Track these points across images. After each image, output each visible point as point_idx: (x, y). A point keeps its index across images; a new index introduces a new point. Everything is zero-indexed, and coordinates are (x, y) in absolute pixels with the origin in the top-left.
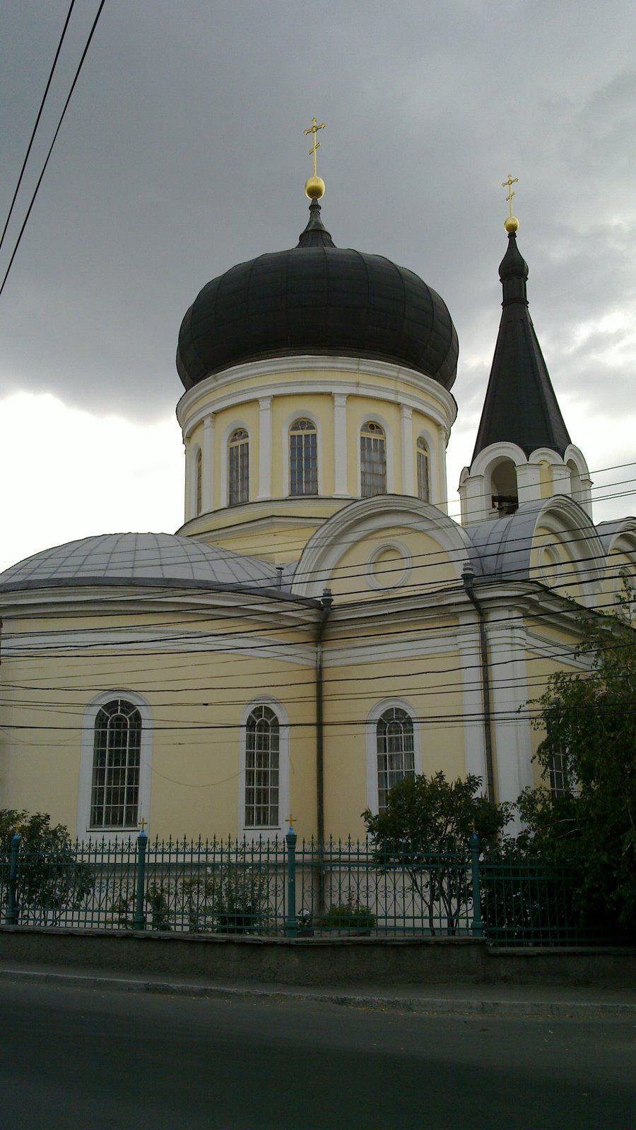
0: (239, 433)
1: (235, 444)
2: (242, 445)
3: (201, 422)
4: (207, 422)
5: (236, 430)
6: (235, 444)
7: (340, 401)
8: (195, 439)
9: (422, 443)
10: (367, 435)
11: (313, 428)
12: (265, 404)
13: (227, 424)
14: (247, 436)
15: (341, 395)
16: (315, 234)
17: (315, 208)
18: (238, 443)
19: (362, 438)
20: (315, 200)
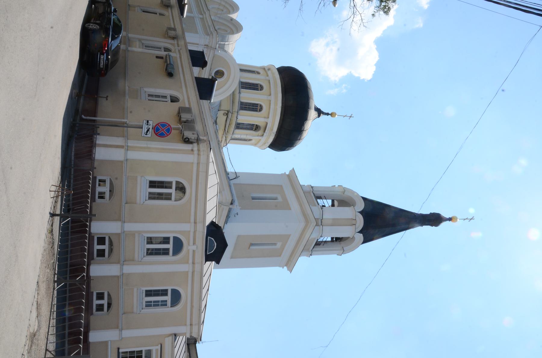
0: (262, 88)
1: (259, 86)
2: (258, 88)
6: (259, 86)
7: (266, 120)
9: (250, 140)
17: (328, 114)
19: (254, 124)
20: (330, 114)
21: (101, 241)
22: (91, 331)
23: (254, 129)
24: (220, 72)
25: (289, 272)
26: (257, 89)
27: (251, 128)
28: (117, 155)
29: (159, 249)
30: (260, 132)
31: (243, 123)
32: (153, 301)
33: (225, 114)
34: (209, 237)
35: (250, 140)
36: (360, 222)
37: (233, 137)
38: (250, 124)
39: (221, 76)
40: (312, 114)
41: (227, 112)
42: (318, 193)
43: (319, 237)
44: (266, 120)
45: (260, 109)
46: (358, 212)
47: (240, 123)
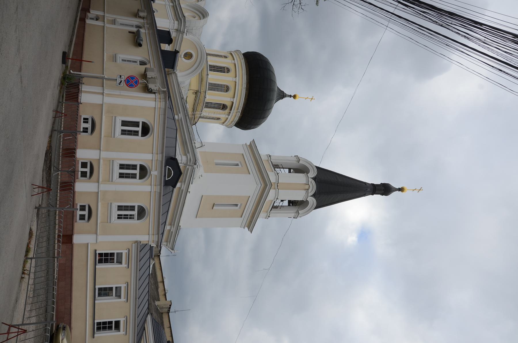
0: (228, 70)
2: (225, 71)
3: (234, 60)
4: (233, 61)
5: (229, 69)
6: (226, 69)
8: (230, 55)
9: (218, 119)
10: (222, 105)
11: (227, 91)
12: (234, 79)
13: (232, 68)
14: (227, 73)
15: (234, 100)
16: (282, 95)
17: (290, 96)
18: (226, 70)
19: (221, 104)
21: (84, 165)
22: (75, 235)
23: (221, 108)
24: (188, 54)
25: (249, 232)
26: (224, 72)
27: (219, 107)
28: (96, 99)
29: (129, 174)
30: (227, 111)
31: (211, 103)
32: (124, 215)
33: (194, 93)
34: (167, 167)
35: (218, 119)
36: (313, 187)
37: (202, 115)
38: (218, 103)
39: (189, 58)
40: (275, 95)
41: (196, 91)
42: (275, 162)
43: (276, 199)
44: (232, 100)
45: (226, 90)
46: (311, 178)
47: (208, 102)
